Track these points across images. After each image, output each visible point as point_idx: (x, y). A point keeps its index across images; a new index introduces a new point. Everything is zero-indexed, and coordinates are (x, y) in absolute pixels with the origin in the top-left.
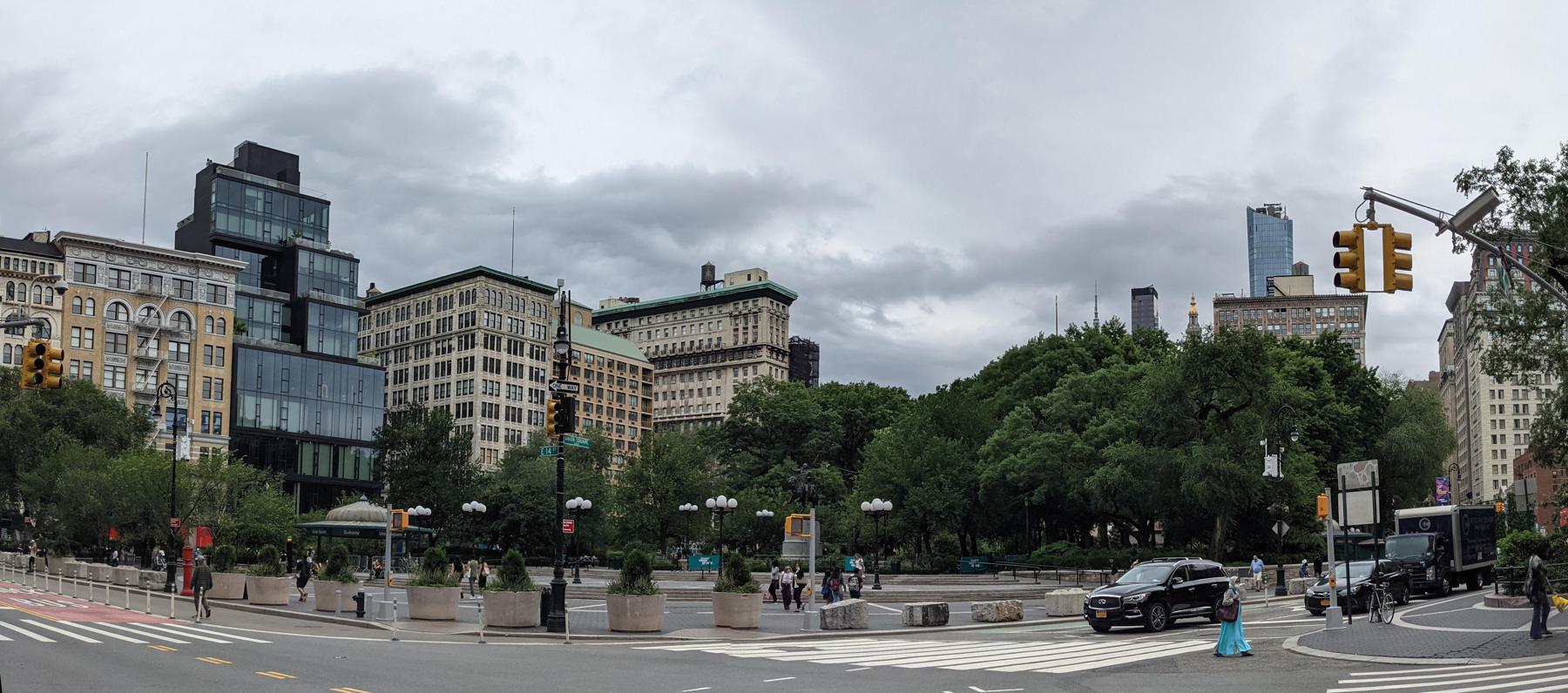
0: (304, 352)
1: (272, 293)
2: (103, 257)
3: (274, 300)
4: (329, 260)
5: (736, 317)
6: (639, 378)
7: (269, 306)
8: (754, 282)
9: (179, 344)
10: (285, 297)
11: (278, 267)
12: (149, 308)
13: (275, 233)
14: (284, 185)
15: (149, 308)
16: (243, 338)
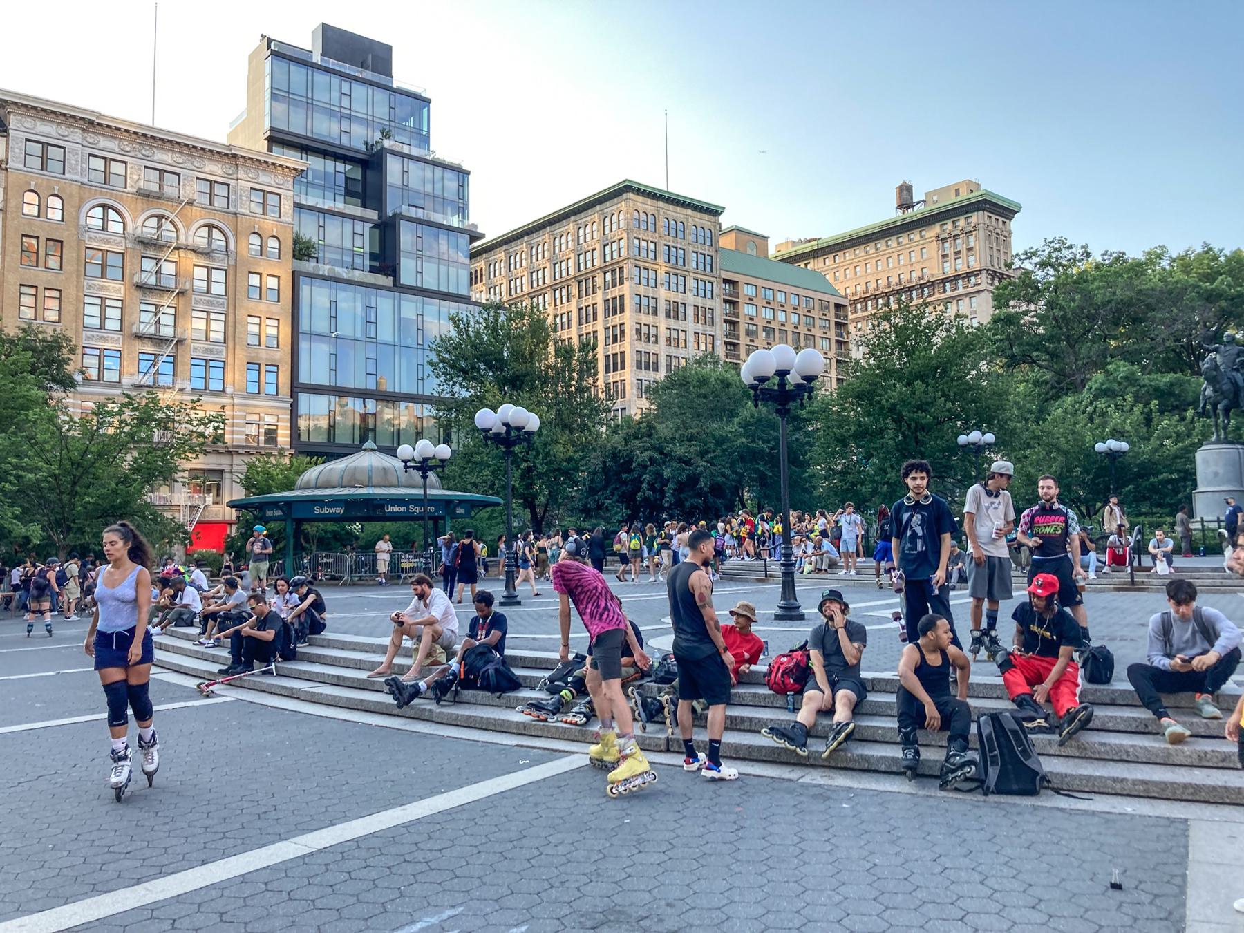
0: (398, 287)
1: (357, 211)
2: (77, 135)
3: (363, 220)
4: (429, 168)
5: (944, 240)
6: (831, 315)
7: (348, 225)
8: (964, 195)
9: (209, 269)
10: (373, 215)
11: (365, 174)
12: (160, 218)
13: (358, 137)
14: (368, 75)
15: (160, 218)
16: (310, 266)
